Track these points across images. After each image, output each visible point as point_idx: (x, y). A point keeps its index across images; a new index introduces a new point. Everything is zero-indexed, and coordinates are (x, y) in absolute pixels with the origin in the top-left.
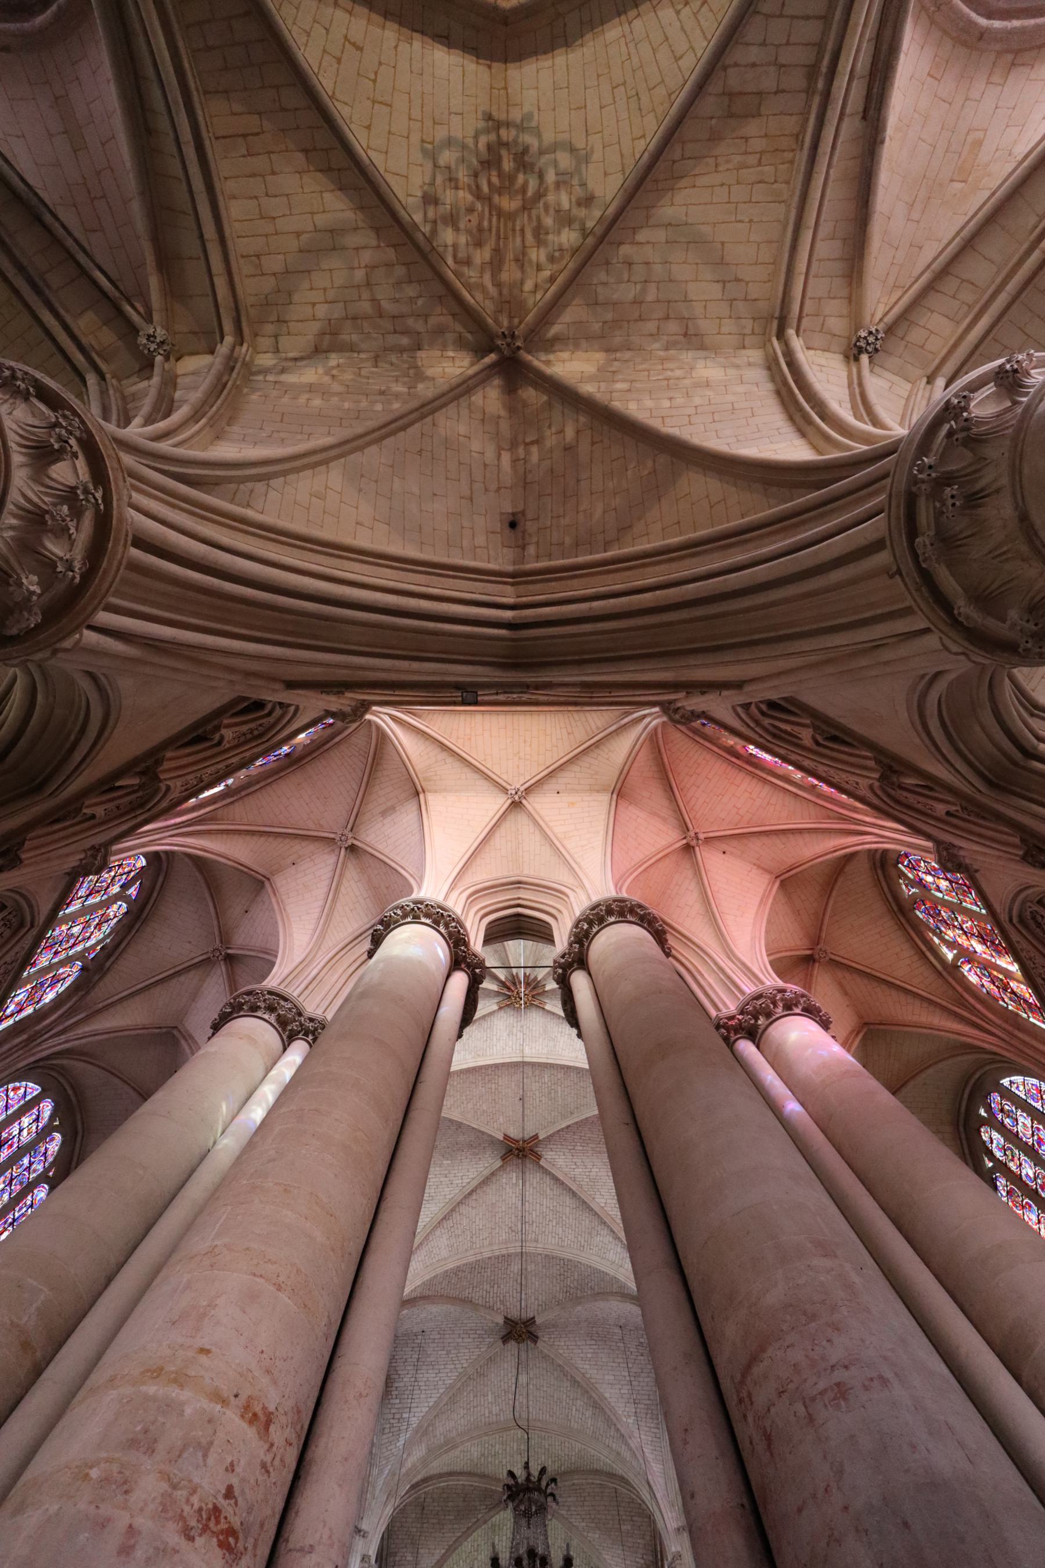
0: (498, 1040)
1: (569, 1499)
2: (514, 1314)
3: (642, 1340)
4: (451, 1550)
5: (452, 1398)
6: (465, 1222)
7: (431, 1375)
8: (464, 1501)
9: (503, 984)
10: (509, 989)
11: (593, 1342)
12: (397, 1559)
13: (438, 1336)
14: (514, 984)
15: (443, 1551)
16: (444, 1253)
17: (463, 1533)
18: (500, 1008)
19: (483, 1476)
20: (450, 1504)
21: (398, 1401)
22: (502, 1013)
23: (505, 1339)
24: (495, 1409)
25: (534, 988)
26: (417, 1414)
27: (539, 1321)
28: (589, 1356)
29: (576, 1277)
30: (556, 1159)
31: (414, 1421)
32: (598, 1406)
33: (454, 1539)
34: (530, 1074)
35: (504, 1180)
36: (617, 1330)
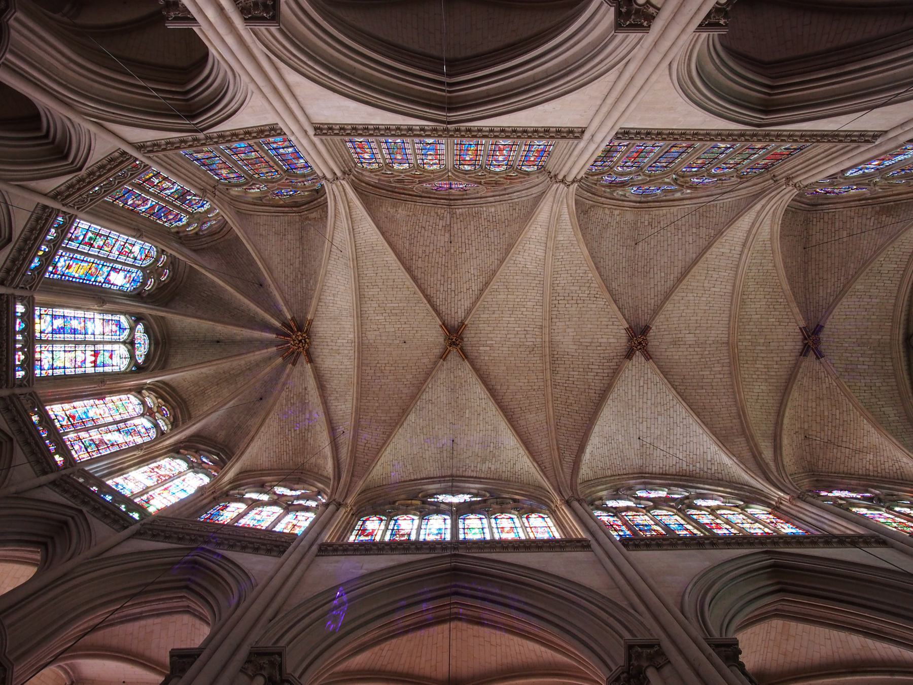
1: (821, 294)
3: (646, 223)
6: (519, 396)
8: (823, 399)
11: (652, 270)
12: (871, 468)
13: (645, 423)
15: (865, 421)
17: (849, 401)
18: (311, 360)
20: (826, 414)
21: (698, 465)
22: (319, 360)
25: (292, 330)
28: (663, 274)
29: (577, 288)
31: (714, 448)
33: (855, 410)
34: (377, 333)
35: (487, 358)
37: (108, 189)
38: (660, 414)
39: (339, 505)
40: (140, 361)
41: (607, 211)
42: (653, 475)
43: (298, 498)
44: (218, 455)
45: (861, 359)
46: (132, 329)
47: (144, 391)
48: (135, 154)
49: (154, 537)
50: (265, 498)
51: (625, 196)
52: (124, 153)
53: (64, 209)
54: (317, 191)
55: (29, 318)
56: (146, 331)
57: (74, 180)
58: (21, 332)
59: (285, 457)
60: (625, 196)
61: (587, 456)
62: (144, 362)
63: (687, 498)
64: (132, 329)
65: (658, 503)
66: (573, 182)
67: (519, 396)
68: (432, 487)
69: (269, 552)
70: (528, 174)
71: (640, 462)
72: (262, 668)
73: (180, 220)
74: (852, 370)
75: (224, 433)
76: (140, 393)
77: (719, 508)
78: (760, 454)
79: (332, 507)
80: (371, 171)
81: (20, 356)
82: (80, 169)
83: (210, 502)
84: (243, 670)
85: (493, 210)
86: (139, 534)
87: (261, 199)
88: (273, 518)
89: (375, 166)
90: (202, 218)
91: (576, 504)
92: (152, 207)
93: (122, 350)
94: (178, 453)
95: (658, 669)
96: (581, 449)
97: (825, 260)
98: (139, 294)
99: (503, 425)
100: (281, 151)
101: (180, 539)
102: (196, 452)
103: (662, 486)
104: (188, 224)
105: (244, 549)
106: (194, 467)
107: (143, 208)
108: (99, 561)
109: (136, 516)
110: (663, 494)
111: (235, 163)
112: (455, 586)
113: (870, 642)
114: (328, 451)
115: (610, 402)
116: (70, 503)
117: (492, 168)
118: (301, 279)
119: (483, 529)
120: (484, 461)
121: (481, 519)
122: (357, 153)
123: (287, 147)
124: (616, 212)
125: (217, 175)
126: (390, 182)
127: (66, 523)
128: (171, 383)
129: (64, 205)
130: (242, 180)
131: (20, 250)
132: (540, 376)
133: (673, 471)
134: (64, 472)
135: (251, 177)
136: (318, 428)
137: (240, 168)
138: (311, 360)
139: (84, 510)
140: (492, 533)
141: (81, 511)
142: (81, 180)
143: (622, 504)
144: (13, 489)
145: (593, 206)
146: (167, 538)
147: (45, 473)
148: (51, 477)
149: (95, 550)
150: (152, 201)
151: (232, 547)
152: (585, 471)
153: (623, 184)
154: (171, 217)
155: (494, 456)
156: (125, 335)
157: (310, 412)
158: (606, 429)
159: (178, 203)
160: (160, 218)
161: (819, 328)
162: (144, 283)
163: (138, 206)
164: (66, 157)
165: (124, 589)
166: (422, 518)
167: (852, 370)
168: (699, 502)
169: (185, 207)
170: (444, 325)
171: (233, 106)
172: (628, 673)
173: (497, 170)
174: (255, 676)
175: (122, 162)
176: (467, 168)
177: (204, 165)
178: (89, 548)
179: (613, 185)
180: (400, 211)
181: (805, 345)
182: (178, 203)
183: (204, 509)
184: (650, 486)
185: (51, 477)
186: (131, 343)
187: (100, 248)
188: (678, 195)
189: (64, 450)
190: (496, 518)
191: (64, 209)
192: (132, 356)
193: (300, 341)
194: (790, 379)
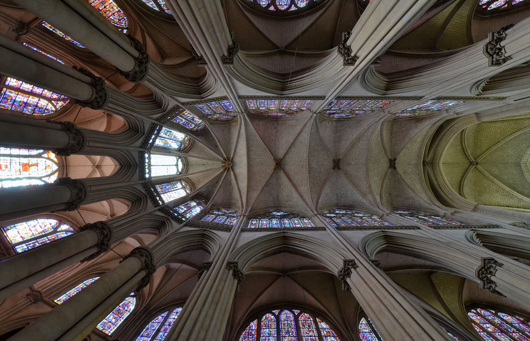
0: (242, 171)
2: (332, 166)
4: (409, 187)
5: (355, 186)
6: (298, 182)
7: (349, 192)
9: (225, 170)
10: (227, 168)
14: (226, 166)
16: (306, 188)
18: (233, 170)
19: (385, 176)
20: (397, 186)
22: (235, 170)
23: (339, 169)
24: (362, 172)
26: (358, 197)
27: (390, 158)
30: (281, 153)
31: (361, 198)
32: (359, 139)
35: (288, 169)
36: (337, 134)
37: (172, 118)
38: (343, 187)
39: (244, 216)
40: (180, 170)
41: (327, 122)
42: (341, 206)
43: (230, 213)
44: (204, 200)
45: (408, 169)
46: (178, 161)
47: (182, 180)
48: (181, 106)
49: (191, 226)
50: (220, 213)
51: (333, 117)
52: (178, 106)
53: (159, 124)
54: (235, 116)
55: (149, 158)
56: (182, 161)
57: (163, 115)
58: (148, 163)
59: (225, 201)
60: (333, 117)
61: (320, 200)
62: (181, 171)
63: (353, 213)
64: (178, 161)
65: (343, 215)
66: (319, 113)
67: (298, 182)
68: (271, 210)
69: (226, 231)
70: (303, 110)
71: (337, 202)
72: (232, 267)
73: (192, 126)
74: (406, 173)
75: (206, 193)
76: (180, 181)
77: (363, 217)
78: (376, 200)
79: (242, 217)
80: (253, 110)
81: (147, 171)
82: (165, 111)
83: (204, 215)
84: (226, 268)
85: (290, 122)
86: (186, 225)
87: (217, 119)
88: (224, 220)
89: (254, 108)
90: (198, 125)
91: (319, 216)
92: (184, 122)
93: (175, 167)
94: (193, 199)
95: (355, 269)
96: (319, 198)
97: (398, 137)
98: (179, 150)
99: (293, 190)
100: (225, 104)
101: (199, 227)
102: (198, 199)
103: (344, 209)
104: (194, 127)
105: (218, 230)
106: (198, 204)
107: (181, 123)
108: (176, 234)
109: (184, 219)
110: (344, 212)
111: (210, 108)
112: (285, 242)
113: (415, 259)
114: (239, 200)
115: (327, 183)
116: (165, 216)
117: (292, 109)
118: (229, 144)
119: (289, 223)
120: (287, 202)
121: (288, 220)
122: (249, 104)
123: (227, 103)
124: (330, 122)
125: (204, 112)
126: (258, 113)
127: (164, 222)
128: (189, 178)
129: (159, 123)
130: (212, 113)
131: (147, 137)
132: (305, 175)
133: (347, 205)
134: (162, 206)
135: (215, 112)
136: (235, 192)
137: (212, 109)
138: (233, 170)
139: (169, 218)
140: (293, 225)
141: (168, 218)
142: (165, 115)
143: (332, 215)
144: (148, 212)
145: (323, 120)
146: (195, 227)
147: (156, 206)
148: (159, 208)
149: (174, 230)
150: (184, 120)
151: (214, 229)
152: (320, 205)
153: (333, 114)
154: (189, 125)
155: (291, 200)
156: (175, 163)
157: (233, 187)
158: (326, 191)
159: (192, 121)
160: (186, 126)
161: (395, 159)
162: (181, 146)
163: (180, 122)
164: (161, 107)
165: (184, 242)
166: (270, 219)
167: (406, 173)
168: (356, 215)
169: (194, 122)
170: (275, 159)
171: (214, 90)
172: (344, 269)
173: (293, 109)
174: (230, 270)
175: (178, 108)
176: (284, 109)
177: (201, 109)
178: (172, 229)
179: (330, 114)
180: (261, 123)
181: (391, 165)
182: (192, 121)
183: (202, 217)
184: (340, 210)
185: (159, 208)
186: (177, 165)
187: (168, 136)
188: (351, 116)
189: (161, 199)
190: (293, 220)
191: (159, 124)
192: (178, 170)
193: (229, 164)
194: (385, 176)
